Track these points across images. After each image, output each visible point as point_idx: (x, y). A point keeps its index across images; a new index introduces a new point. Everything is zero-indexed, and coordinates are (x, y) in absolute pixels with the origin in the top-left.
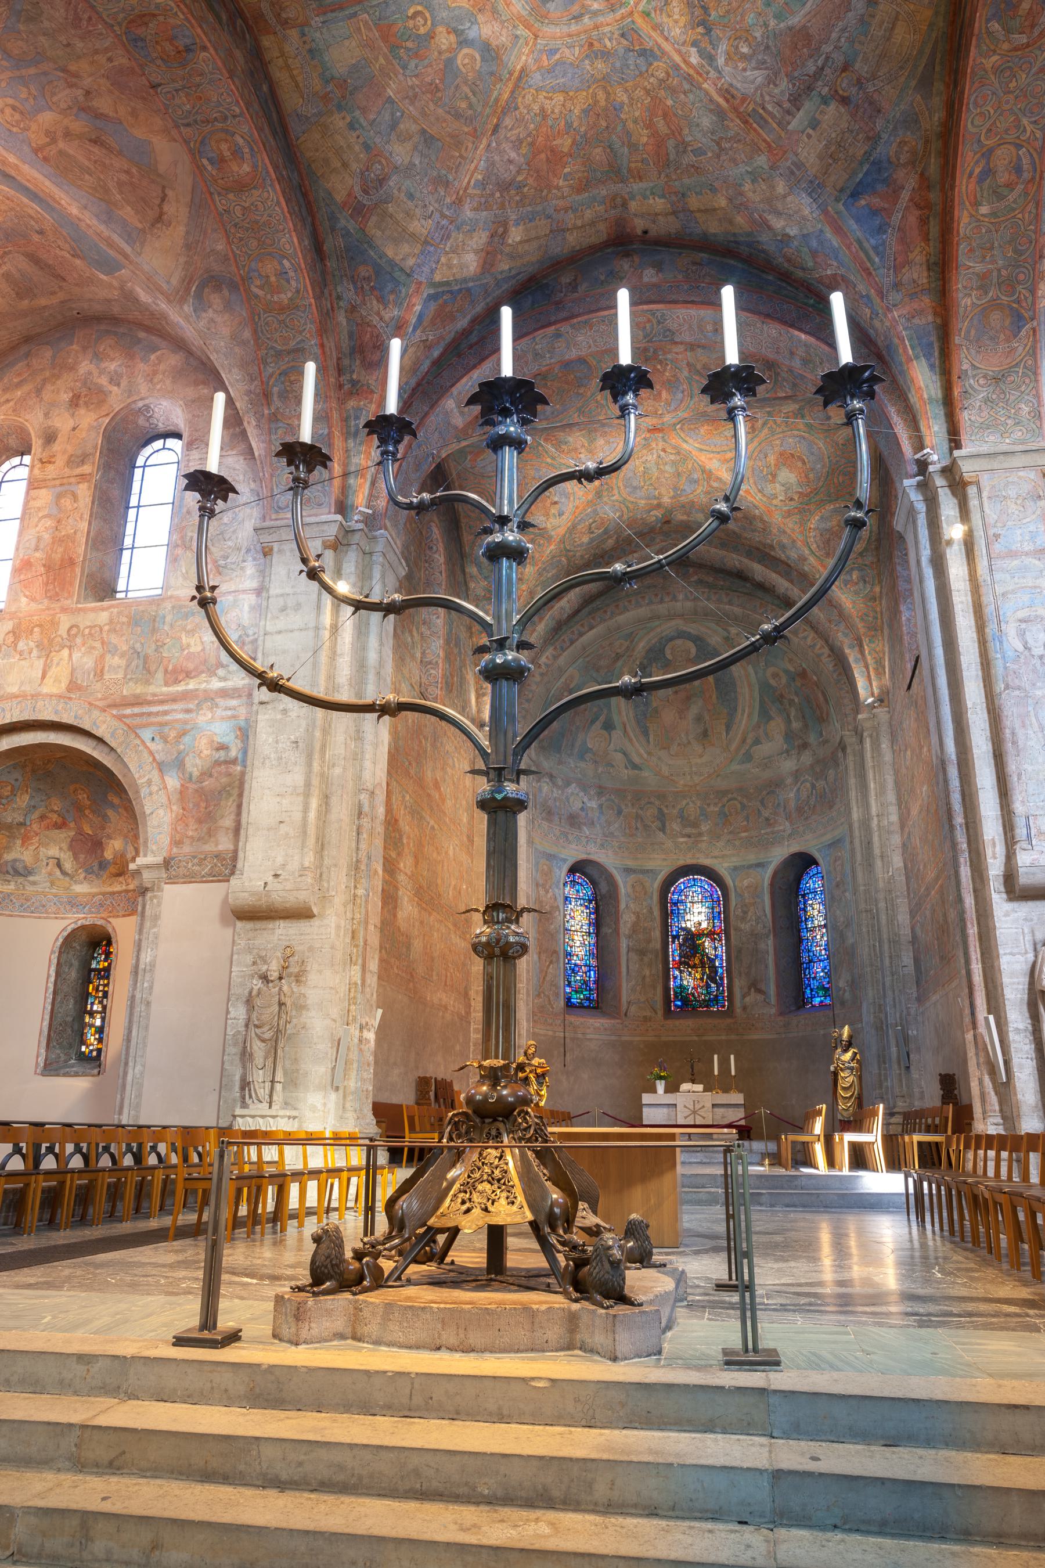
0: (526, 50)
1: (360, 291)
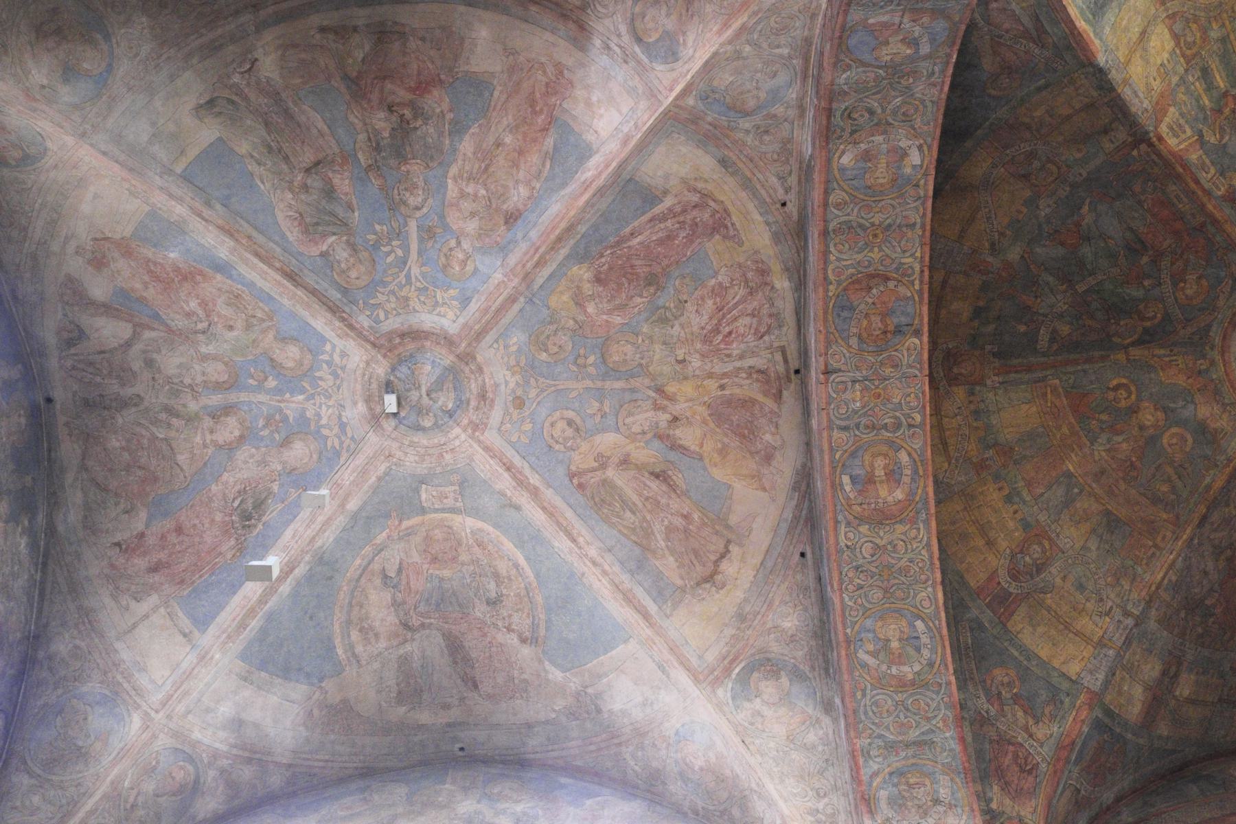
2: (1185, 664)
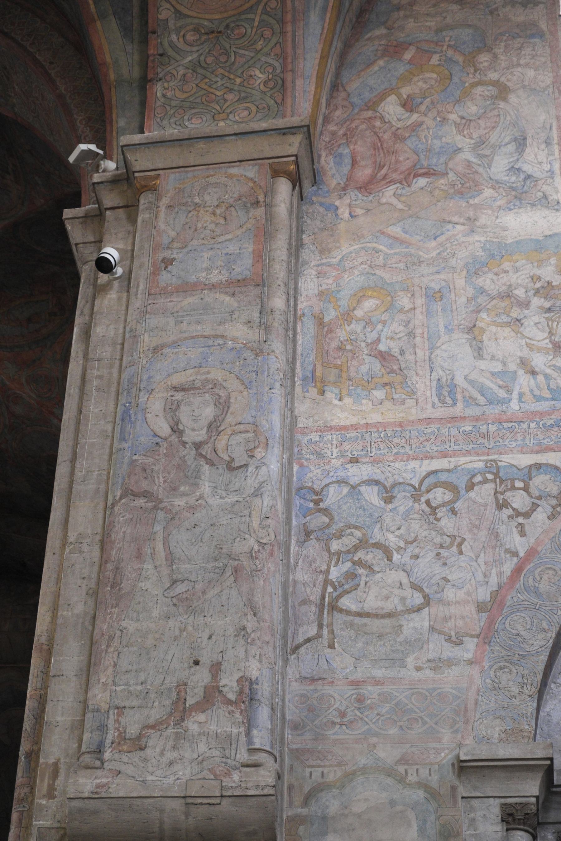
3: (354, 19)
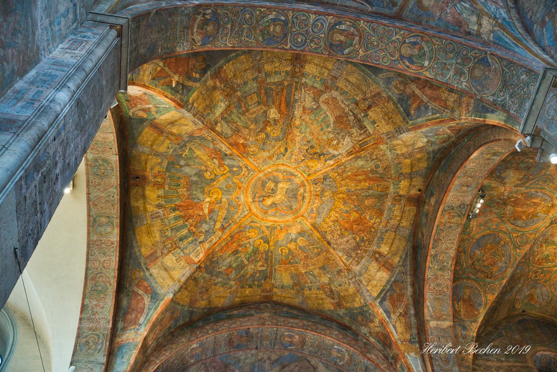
0: (305, 221)
1: (366, 326)
2: (377, 249)
3: (527, 34)
